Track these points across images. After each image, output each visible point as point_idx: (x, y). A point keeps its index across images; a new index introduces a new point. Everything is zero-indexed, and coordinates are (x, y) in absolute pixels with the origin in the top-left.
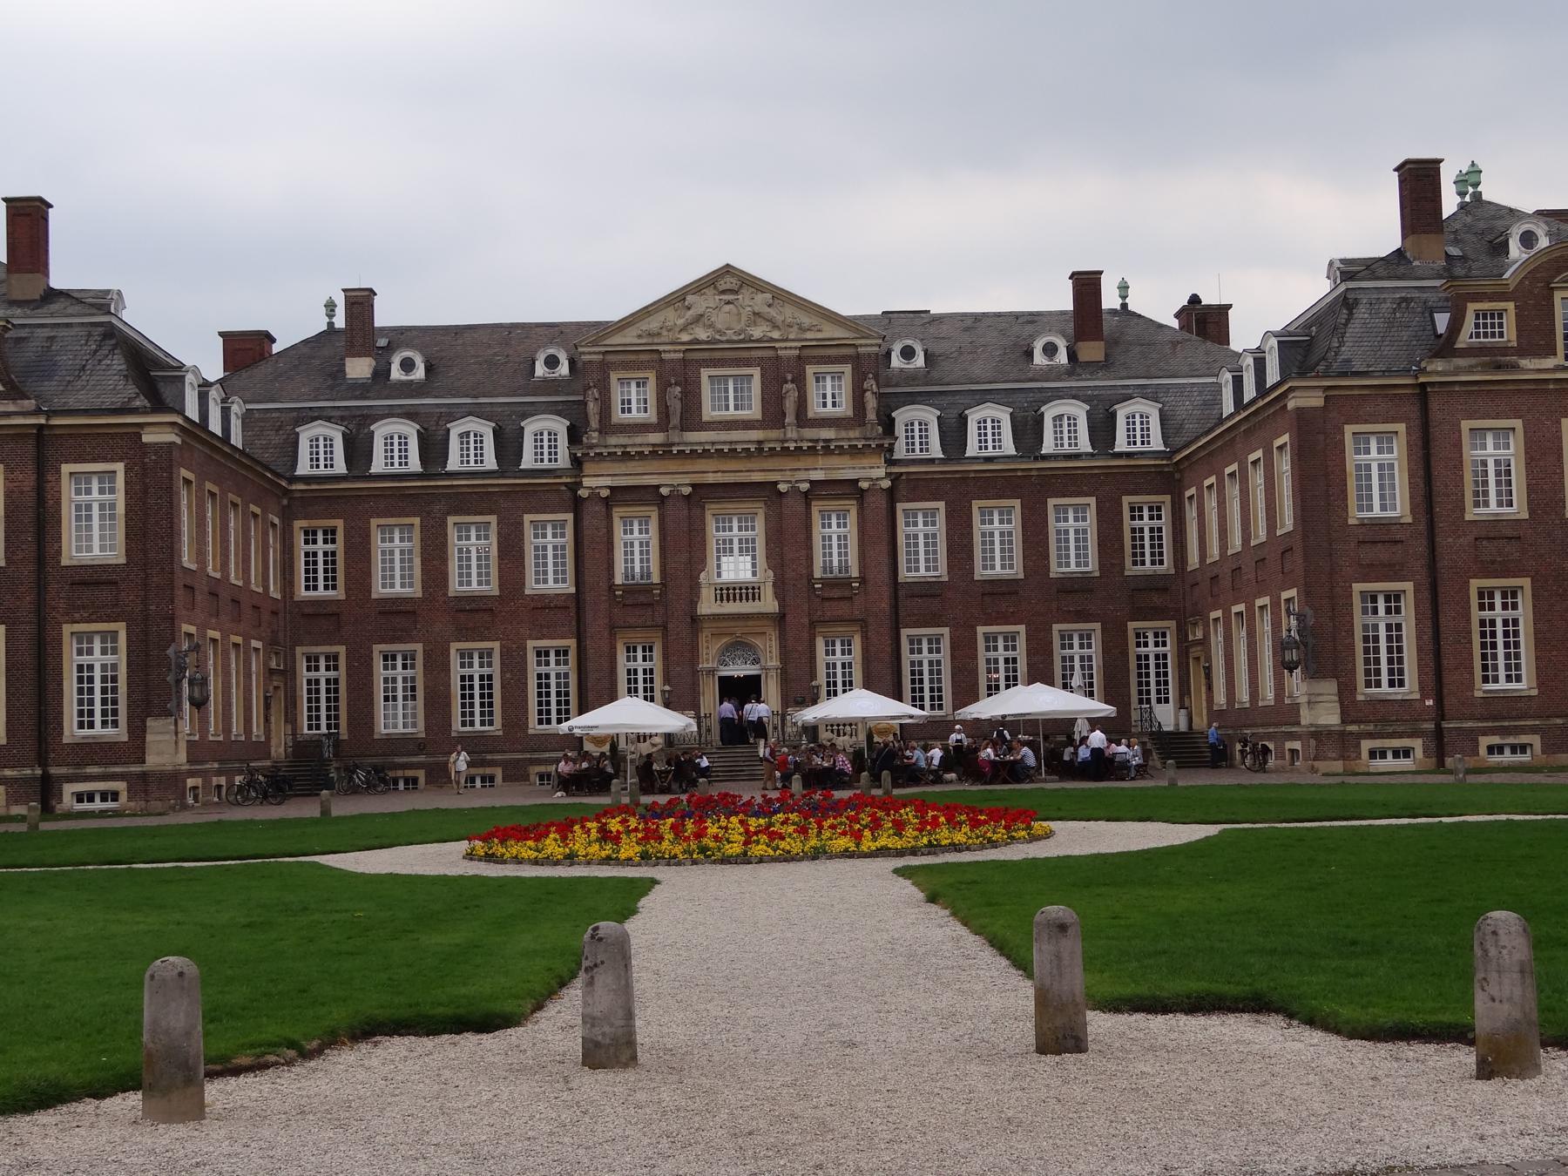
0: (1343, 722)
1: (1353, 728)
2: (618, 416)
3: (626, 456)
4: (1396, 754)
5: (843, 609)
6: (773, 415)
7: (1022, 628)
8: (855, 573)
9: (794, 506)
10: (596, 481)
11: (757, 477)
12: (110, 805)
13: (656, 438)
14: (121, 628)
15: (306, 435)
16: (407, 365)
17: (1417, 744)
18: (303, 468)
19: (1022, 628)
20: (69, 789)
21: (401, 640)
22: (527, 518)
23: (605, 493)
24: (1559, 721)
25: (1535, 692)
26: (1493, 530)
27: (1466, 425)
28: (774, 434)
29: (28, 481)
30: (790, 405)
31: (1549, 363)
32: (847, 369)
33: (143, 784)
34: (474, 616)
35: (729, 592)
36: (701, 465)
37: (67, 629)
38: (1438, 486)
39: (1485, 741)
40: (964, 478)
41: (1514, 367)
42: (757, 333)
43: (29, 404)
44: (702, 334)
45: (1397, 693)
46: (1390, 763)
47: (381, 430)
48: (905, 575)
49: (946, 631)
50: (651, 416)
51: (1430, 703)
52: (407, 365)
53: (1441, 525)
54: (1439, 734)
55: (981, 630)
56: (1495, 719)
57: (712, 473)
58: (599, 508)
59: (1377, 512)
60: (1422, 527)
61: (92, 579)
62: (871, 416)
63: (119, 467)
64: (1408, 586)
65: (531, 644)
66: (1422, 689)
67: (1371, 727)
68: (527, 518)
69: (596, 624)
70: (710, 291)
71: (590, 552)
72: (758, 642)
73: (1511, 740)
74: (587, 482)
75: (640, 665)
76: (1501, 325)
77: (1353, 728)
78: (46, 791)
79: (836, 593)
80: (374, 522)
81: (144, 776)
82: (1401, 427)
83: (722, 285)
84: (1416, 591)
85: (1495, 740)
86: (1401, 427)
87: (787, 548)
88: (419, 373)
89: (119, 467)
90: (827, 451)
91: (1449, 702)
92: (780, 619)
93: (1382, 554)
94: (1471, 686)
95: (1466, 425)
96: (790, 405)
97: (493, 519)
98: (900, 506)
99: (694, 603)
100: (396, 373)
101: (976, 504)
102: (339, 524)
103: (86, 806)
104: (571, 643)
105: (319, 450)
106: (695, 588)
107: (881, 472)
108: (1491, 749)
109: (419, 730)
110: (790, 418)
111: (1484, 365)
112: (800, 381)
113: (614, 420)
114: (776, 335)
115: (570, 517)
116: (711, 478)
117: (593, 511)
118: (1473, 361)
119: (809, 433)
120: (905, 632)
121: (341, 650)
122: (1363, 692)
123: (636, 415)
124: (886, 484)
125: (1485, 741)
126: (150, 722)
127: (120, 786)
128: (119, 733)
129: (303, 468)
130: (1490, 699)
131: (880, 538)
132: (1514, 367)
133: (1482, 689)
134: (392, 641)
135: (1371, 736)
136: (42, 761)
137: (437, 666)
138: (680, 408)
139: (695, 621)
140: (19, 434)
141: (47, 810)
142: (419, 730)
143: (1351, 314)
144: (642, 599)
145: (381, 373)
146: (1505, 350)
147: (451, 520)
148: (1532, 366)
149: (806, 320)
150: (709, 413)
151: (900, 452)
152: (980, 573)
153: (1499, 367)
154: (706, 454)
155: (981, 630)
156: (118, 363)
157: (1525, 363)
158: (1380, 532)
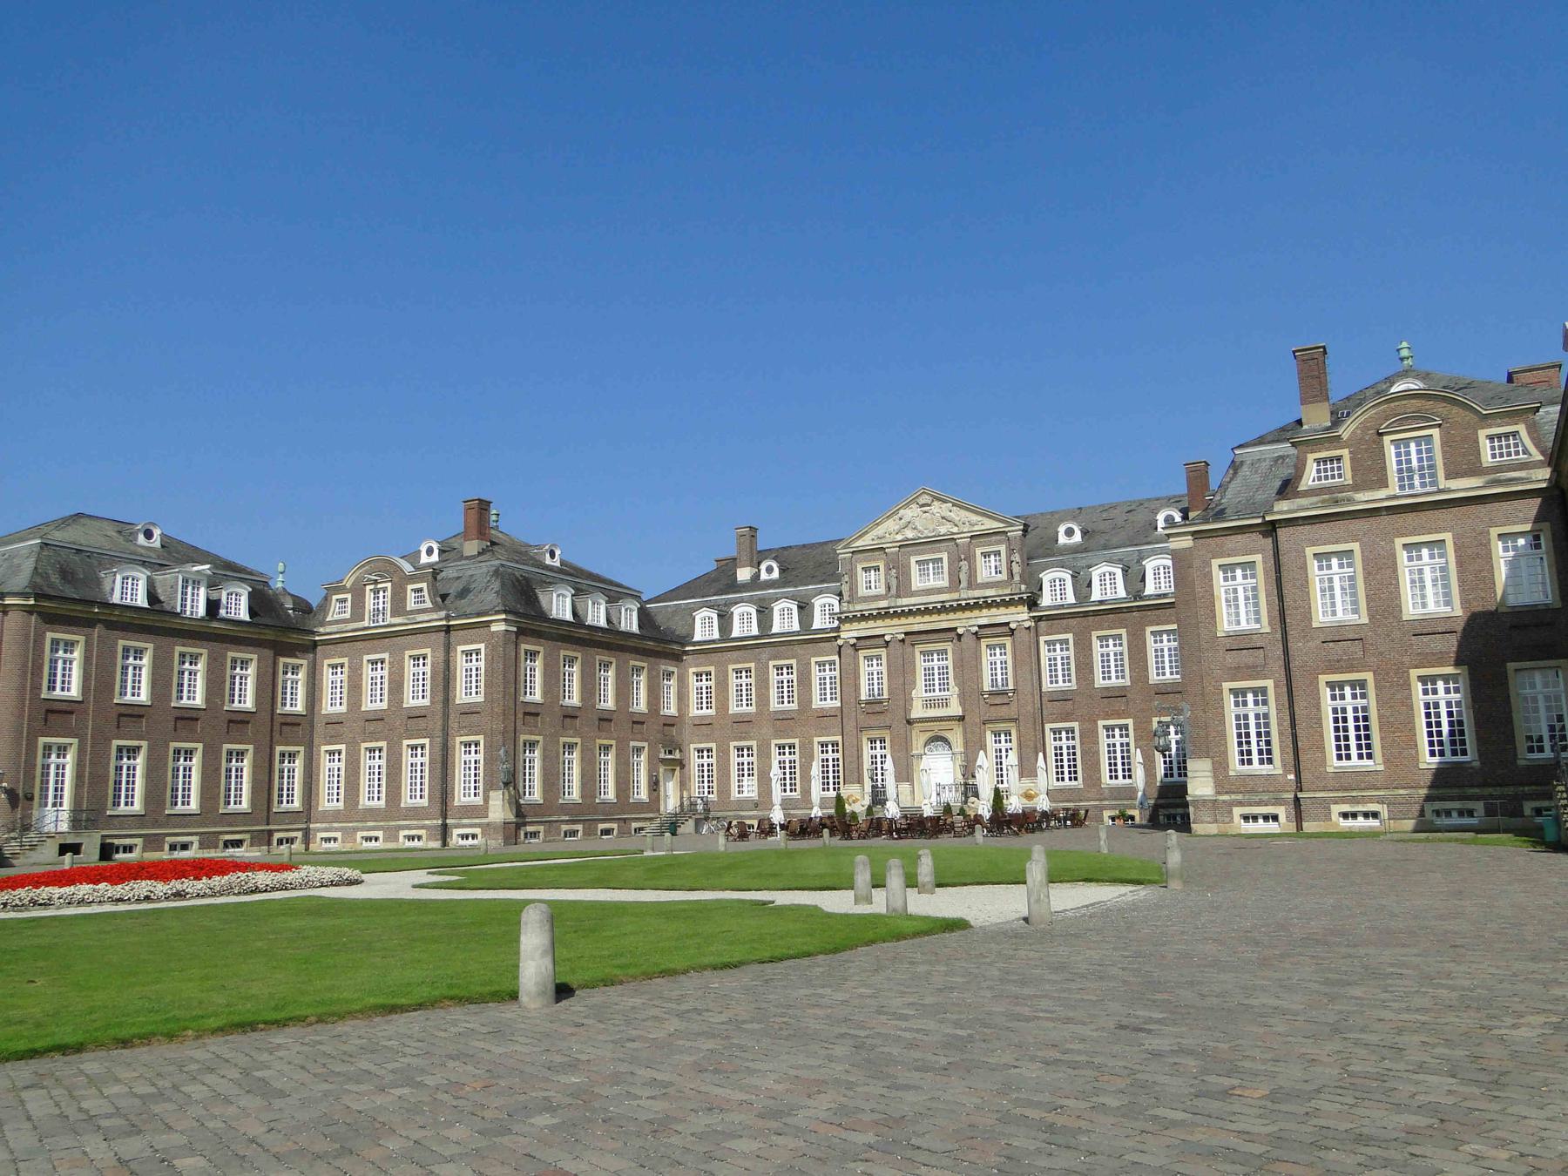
0: (1218, 793)
1: (1226, 797)
2: (862, 591)
3: (864, 618)
4: (1266, 818)
5: (1003, 712)
6: (955, 584)
7: (1130, 722)
8: (1011, 687)
9: (968, 641)
10: (849, 633)
11: (945, 625)
12: (475, 842)
13: (883, 604)
14: (481, 738)
15: (700, 616)
16: (770, 570)
17: (1281, 811)
18: (697, 638)
19: (1130, 722)
20: (456, 832)
21: (744, 739)
22: (813, 660)
23: (853, 641)
24: (1402, 792)
25: (1381, 768)
26: (1337, 636)
27: (1310, 551)
28: (955, 596)
29: (441, 655)
30: (963, 577)
31: (1382, 494)
32: (1003, 548)
33: (487, 828)
34: (784, 722)
35: (930, 703)
36: (911, 620)
37: (458, 740)
38: (1288, 601)
39: (1336, 809)
40: (1086, 614)
41: (1350, 501)
42: (943, 530)
43: (443, 614)
44: (910, 534)
45: (1266, 769)
46: (1261, 827)
47: (737, 611)
48: (1047, 686)
49: (1075, 725)
50: (882, 590)
51: (1291, 777)
52: (770, 570)
53: (1292, 633)
54: (1297, 800)
55: (1101, 723)
56: (1346, 790)
57: (918, 623)
58: (850, 651)
59: (1244, 625)
60: (1279, 636)
61: (470, 711)
62: (1017, 578)
63: (482, 646)
64: (1269, 683)
65: (816, 739)
66: (1284, 766)
67: (1240, 797)
68: (813, 660)
69: (850, 726)
70: (914, 506)
71: (849, 679)
72: (948, 735)
73: (1360, 808)
74: (843, 635)
75: (878, 752)
76: (1339, 468)
77: (1226, 797)
78: (445, 832)
79: (998, 700)
80: (731, 667)
81: (488, 824)
82: (1258, 558)
83: (921, 501)
84: (1276, 687)
85: (1346, 808)
86: (1258, 558)
87: (967, 669)
88: (776, 574)
89: (482, 646)
90: (988, 606)
91: (1305, 775)
92: (962, 719)
93: (1246, 658)
94: (1323, 762)
95: (1310, 551)
96: (963, 577)
97: (793, 662)
98: (1042, 639)
99: (907, 709)
100: (764, 576)
101: (1095, 634)
102: (712, 669)
103: (465, 842)
104: (839, 739)
105: (704, 626)
106: (908, 701)
107: (1026, 616)
108: (1345, 815)
109: (754, 795)
110: (964, 584)
111: (1323, 501)
112: (970, 558)
113: (860, 594)
114: (955, 530)
115: (836, 658)
116: (916, 628)
117: (847, 651)
118: (1315, 499)
119: (977, 593)
120: (1048, 726)
121: (713, 746)
122: (1235, 767)
123: (873, 592)
124: (1027, 624)
125: (1336, 809)
126: (492, 794)
127: (477, 831)
128: (479, 800)
129: (697, 638)
130: (1339, 774)
131: (1028, 661)
132: (1350, 501)
133: (1333, 763)
134: (741, 739)
135: (1241, 804)
136: (445, 817)
137: (764, 755)
138: (901, 585)
139: (909, 722)
140: (437, 629)
141: (445, 844)
142: (754, 795)
143: (1235, 473)
144: (877, 708)
145: (757, 575)
146: (1342, 488)
147: (771, 663)
148: (1365, 499)
149: (974, 518)
150: (917, 583)
151: (1046, 600)
152: (1100, 682)
153: (1336, 502)
154: (911, 613)
155: (1101, 723)
156: (496, 585)
157: (1360, 496)
158: (1242, 643)
